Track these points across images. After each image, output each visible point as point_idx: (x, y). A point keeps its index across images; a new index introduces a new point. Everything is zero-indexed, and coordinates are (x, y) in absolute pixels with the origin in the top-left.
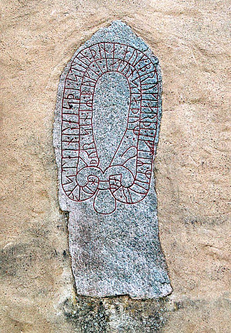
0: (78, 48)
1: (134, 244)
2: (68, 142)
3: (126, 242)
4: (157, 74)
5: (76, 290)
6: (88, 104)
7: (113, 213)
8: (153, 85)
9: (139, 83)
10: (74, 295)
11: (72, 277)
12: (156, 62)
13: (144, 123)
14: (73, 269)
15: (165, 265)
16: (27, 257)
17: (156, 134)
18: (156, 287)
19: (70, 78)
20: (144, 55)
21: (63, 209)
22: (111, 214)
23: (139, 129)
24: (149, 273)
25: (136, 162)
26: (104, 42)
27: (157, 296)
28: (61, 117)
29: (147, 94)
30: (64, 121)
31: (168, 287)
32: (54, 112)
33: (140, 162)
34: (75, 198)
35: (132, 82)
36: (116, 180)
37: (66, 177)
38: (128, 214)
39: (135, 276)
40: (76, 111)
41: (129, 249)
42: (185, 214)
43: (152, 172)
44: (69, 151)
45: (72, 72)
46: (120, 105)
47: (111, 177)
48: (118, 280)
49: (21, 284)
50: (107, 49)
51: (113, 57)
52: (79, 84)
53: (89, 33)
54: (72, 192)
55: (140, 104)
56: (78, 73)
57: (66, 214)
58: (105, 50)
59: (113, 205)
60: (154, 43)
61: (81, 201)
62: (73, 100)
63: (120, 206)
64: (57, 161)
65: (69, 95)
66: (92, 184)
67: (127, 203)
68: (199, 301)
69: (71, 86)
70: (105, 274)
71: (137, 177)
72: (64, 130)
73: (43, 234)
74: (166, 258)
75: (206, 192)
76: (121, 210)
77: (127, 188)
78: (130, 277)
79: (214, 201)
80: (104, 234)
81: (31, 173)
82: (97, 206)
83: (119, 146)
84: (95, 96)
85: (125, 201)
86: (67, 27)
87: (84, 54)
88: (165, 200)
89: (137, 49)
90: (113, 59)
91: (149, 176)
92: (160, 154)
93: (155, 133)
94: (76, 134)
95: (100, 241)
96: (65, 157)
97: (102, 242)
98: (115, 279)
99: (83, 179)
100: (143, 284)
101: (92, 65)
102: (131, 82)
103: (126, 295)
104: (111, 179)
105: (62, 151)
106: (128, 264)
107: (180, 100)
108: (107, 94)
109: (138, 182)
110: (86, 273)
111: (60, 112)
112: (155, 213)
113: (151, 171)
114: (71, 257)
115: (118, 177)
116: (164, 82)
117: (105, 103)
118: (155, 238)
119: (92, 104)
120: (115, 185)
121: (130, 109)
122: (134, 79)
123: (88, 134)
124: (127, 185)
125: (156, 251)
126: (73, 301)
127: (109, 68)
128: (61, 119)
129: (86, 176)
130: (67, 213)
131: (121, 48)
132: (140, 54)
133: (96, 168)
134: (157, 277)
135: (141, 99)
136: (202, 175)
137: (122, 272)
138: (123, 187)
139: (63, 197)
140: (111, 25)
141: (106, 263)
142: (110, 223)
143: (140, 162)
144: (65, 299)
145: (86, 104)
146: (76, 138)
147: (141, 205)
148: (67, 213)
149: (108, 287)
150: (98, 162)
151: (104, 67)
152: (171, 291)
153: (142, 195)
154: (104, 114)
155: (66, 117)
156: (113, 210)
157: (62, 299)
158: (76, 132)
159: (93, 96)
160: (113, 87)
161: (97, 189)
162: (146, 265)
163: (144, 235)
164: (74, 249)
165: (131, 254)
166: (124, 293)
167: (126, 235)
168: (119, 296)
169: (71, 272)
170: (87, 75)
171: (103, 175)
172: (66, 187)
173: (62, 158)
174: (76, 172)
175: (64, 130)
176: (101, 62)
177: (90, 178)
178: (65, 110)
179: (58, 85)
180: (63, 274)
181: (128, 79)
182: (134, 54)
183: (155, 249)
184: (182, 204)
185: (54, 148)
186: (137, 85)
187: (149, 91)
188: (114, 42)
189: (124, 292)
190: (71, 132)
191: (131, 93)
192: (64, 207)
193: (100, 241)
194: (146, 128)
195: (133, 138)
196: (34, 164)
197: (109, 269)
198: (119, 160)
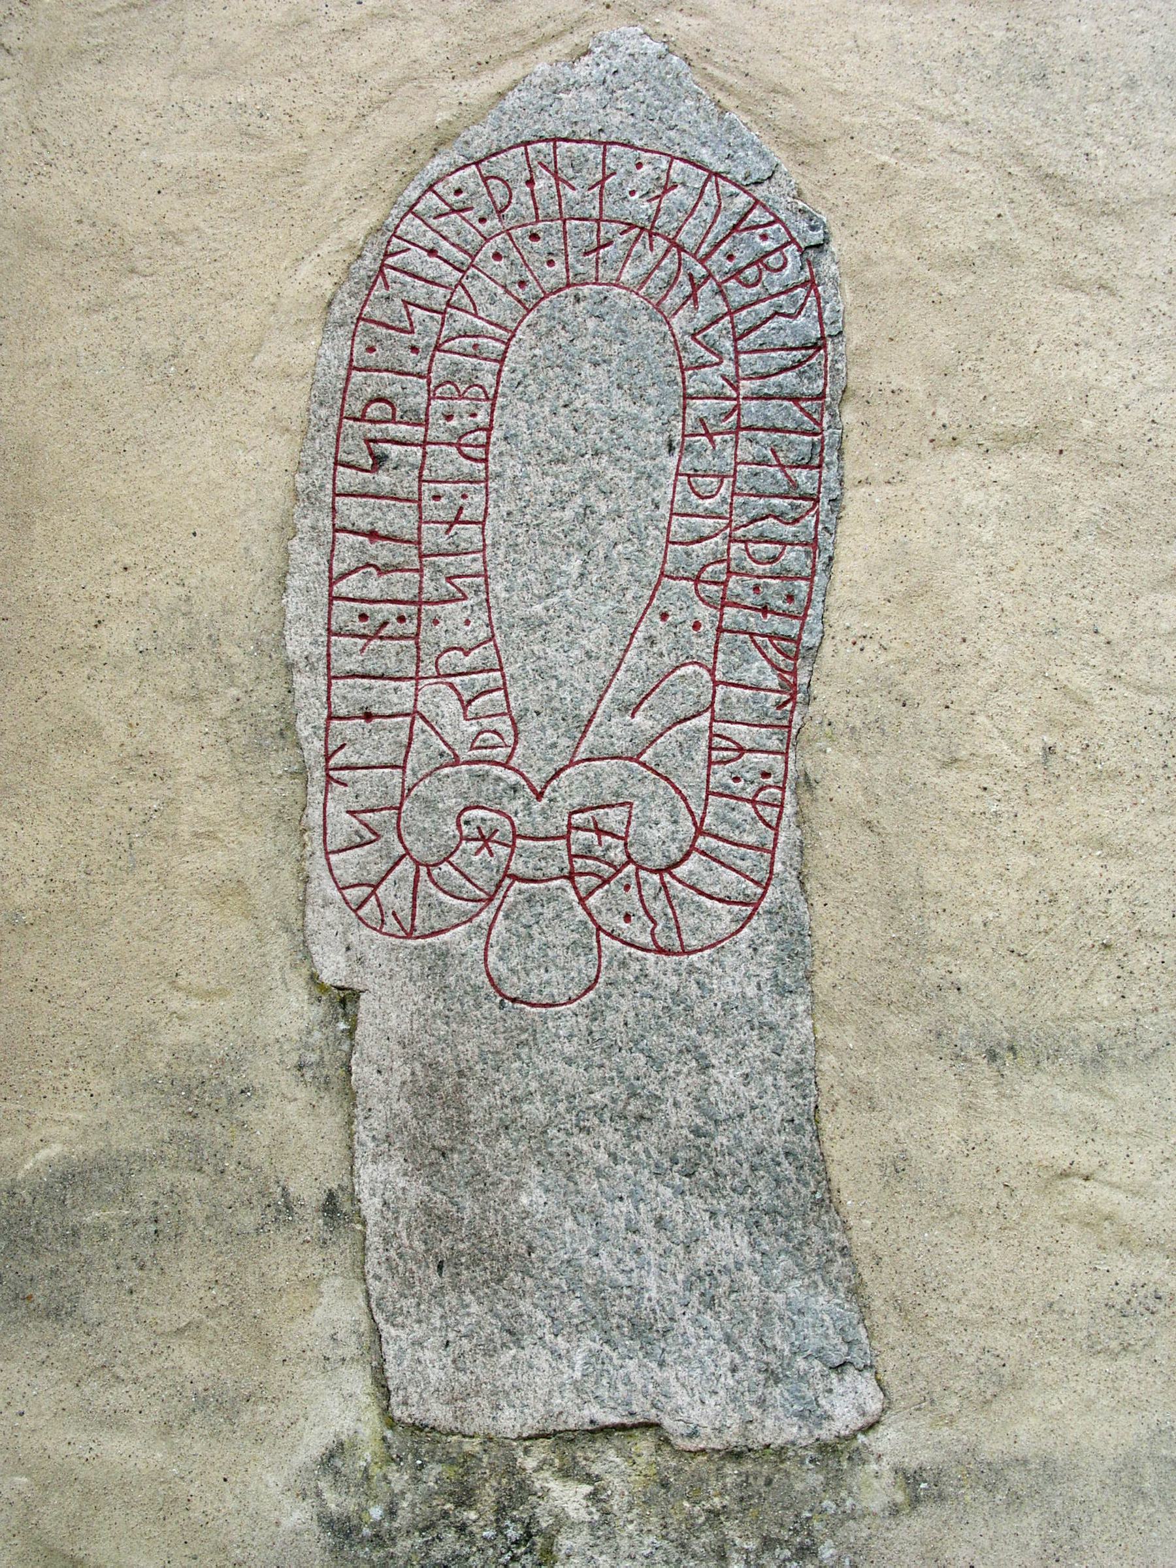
0: (423, 166)
1: (691, 1164)
2: (363, 636)
3: (646, 1151)
4: (818, 298)
5: (387, 1395)
6: (466, 450)
7: (585, 999)
8: (799, 355)
9: (728, 344)
10: (372, 1415)
11: (364, 1326)
12: (816, 237)
13: (752, 547)
14: (375, 1286)
15: (847, 1271)
16: (135, 1223)
17: (810, 600)
18: (804, 1387)
19: (378, 315)
20: (757, 201)
21: (327, 977)
22: (574, 1006)
23: (723, 578)
24: (765, 1312)
25: (704, 744)
26: (555, 140)
27: (805, 1432)
28: (327, 510)
29: (769, 397)
30: (344, 530)
31: (860, 1387)
32: (295, 490)
33: (724, 743)
34: (391, 925)
35: (693, 336)
36: (600, 832)
37: (352, 813)
38: (659, 1005)
39: (691, 1330)
40: (409, 484)
41: (661, 1189)
42: (956, 1012)
43: (788, 793)
44: (366, 681)
45: (387, 286)
46: (627, 455)
47: (578, 819)
48: (606, 1348)
49: (101, 1359)
50: (570, 172)
51: (595, 214)
52: (421, 345)
53: (478, 89)
54: (373, 893)
55: (729, 451)
56: (419, 291)
57: (343, 1002)
58: (557, 179)
59: (583, 959)
60: (806, 145)
61: (424, 936)
62: (391, 426)
63: (623, 964)
64: (305, 732)
65: (372, 401)
66: (479, 850)
67: (660, 951)
68: (1025, 1462)
69: (379, 357)
70: (540, 1316)
71: (707, 820)
72: (343, 576)
73: (224, 1101)
74: (853, 1233)
75: (1063, 898)
76: (624, 988)
77: (658, 871)
78: (667, 1331)
79: (1106, 946)
80: (536, 1110)
81: (167, 793)
82: (501, 967)
83: (621, 660)
84: (503, 408)
85: (645, 939)
86: (369, 59)
87: (452, 198)
88: (853, 937)
89: (717, 174)
90: (598, 221)
91: (770, 813)
92: (828, 699)
93: (803, 596)
94: (402, 596)
95: (516, 1143)
96: (342, 712)
97: (522, 1148)
98: (590, 1342)
99: (430, 829)
100: (734, 1370)
101: (489, 249)
102: (687, 338)
103: (647, 1425)
104: (578, 828)
105: (329, 685)
106: (659, 1266)
107: (933, 431)
108: (565, 396)
109: (714, 843)
110: (438, 1311)
111: (322, 487)
112: (802, 1004)
113: (783, 789)
114: (364, 1223)
115: (613, 819)
116: (855, 337)
117: (553, 442)
118: (799, 1130)
119: (486, 446)
120: (597, 859)
121: (677, 474)
122: (702, 320)
123: (465, 598)
124: (659, 861)
125: (797, 1199)
126: (367, 1454)
127: (580, 269)
128: (328, 522)
129: (449, 810)
130: (345, 1000)
131: (639, 166)
132: (737, 200)
133: (497, 771)
134: (809, 1332)
135: (739, 428)
136: (1044, 813)
137: (626, 1307)
138: (639, 867)
139: (331, 914)
140: (588, 52)
141: (543, 1260)
142: (569, 1049)
143: (724, 743)
144: (329, 1440)
145: (459, 446)
146: (401, 619)
147: (730, 960)
148: (345, 1000)
149: (549, 1381)
150: (510, 741)
151: (551, 263)
152: (879, 1406)
153: (736, 908)
154: (546, 497)
155: (353, 511)
156: (586, 983)
157: (314, 1443)
158: (401, 585)
159: (493, 405)
160: (596, 364)
161: (506, 875)
162: (748, 1271)
163: (741, 1116)
164: (380, 1180)
165: (675, 1212)
166: (632, 1414)
167: (647, 1113)
168: (607, 1431)
169: (363, 1304)
170: (466, 300)
171: (537, 807)
172: (348, 865)
173: (330, 717)
174: (398, 792)
175: (343, 576)
176: (534, 237)
177: (467, 823)
178: (348, 478)
179: (319, 352)
180: (319, 1311)
181: (674, 321)
182: (705, 197)
183: (796, 1192)
184: (940, 959)
185: (290, 667)
186: (719, 355)
187: (780, 386)
188: (603, 137)
189: (635, 1408)
190: (375, 586)
191: (686, 397)
192: (333, 968)
193: (516, 1143)
194: (760, 569)
195: (690, 623)
196: (189, 746)
197: (557, 1287)
198: (617, 731)
